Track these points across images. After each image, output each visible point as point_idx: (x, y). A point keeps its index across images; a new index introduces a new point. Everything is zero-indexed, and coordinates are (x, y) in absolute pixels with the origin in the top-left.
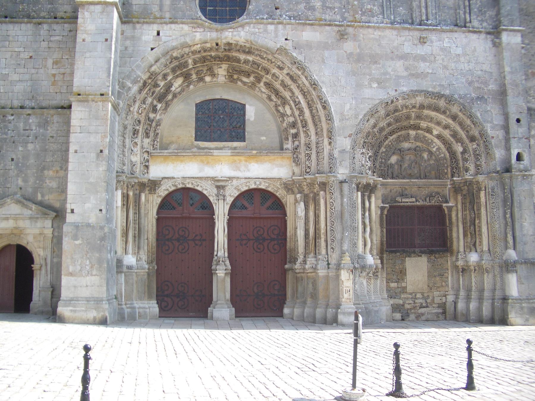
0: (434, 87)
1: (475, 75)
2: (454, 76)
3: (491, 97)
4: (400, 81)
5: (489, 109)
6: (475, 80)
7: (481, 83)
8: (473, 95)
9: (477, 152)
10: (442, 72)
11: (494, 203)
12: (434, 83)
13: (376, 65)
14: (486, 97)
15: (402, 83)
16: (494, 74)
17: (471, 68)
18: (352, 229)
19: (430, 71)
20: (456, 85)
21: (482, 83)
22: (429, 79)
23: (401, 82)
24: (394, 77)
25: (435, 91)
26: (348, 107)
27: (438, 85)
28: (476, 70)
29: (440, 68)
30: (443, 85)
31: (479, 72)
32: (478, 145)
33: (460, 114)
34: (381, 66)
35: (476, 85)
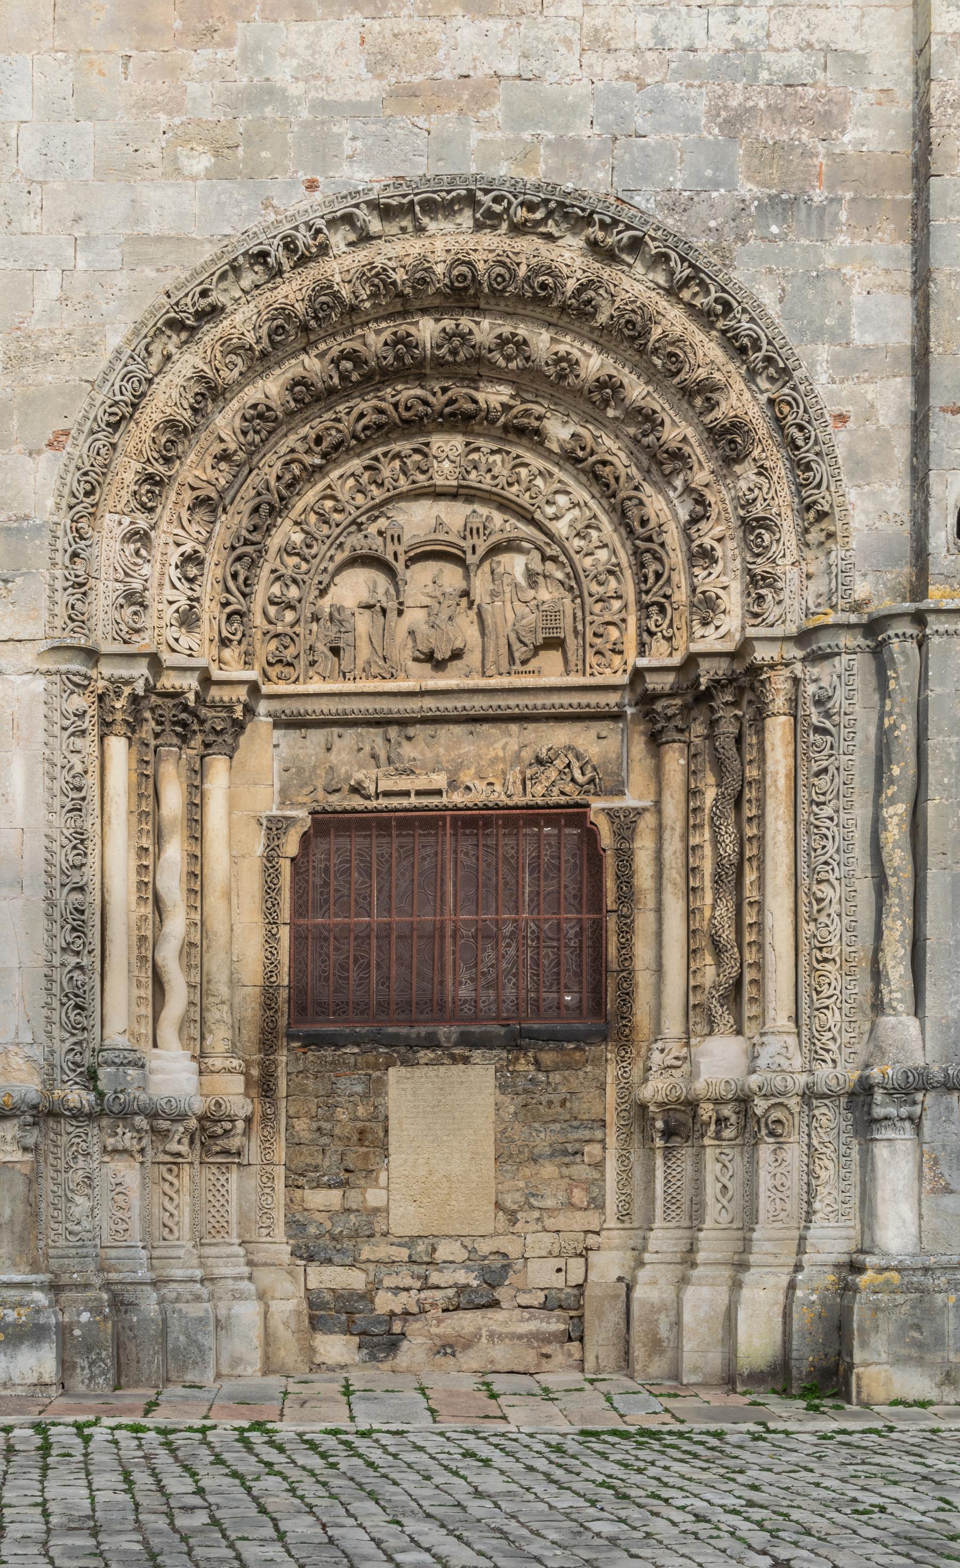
0: (527, 156)
1: (764, 75)
2: (642, 86)
3: (849, 195)
4: (335, 129)
5: (830, 262)
6: (762, 105)
7: (795, 121)
8: (748, 189)
9: (758, 510)
10: (574, 68)
11: (825, 770)
12: (526, 136)
13: (207, 53)
14: (819, 195)
15: (346, 141)
16: (876, 66)
17: (746, 36)
18: (57, 916)
19: (511, 68)
20: (652, 140)
21: (802, 116)
22: (497, 110)
23: (340, 136)
24: (305, 114)
25: (531, 179)
26: (55, 293)
27: (549, 144)
28: (771, 48)
29: (568, 42)
30: (576, 144)
31: (794, 59)
32: (762, 471)
33: (663, 304)
34: (235, 52)
35: (767, 131)
